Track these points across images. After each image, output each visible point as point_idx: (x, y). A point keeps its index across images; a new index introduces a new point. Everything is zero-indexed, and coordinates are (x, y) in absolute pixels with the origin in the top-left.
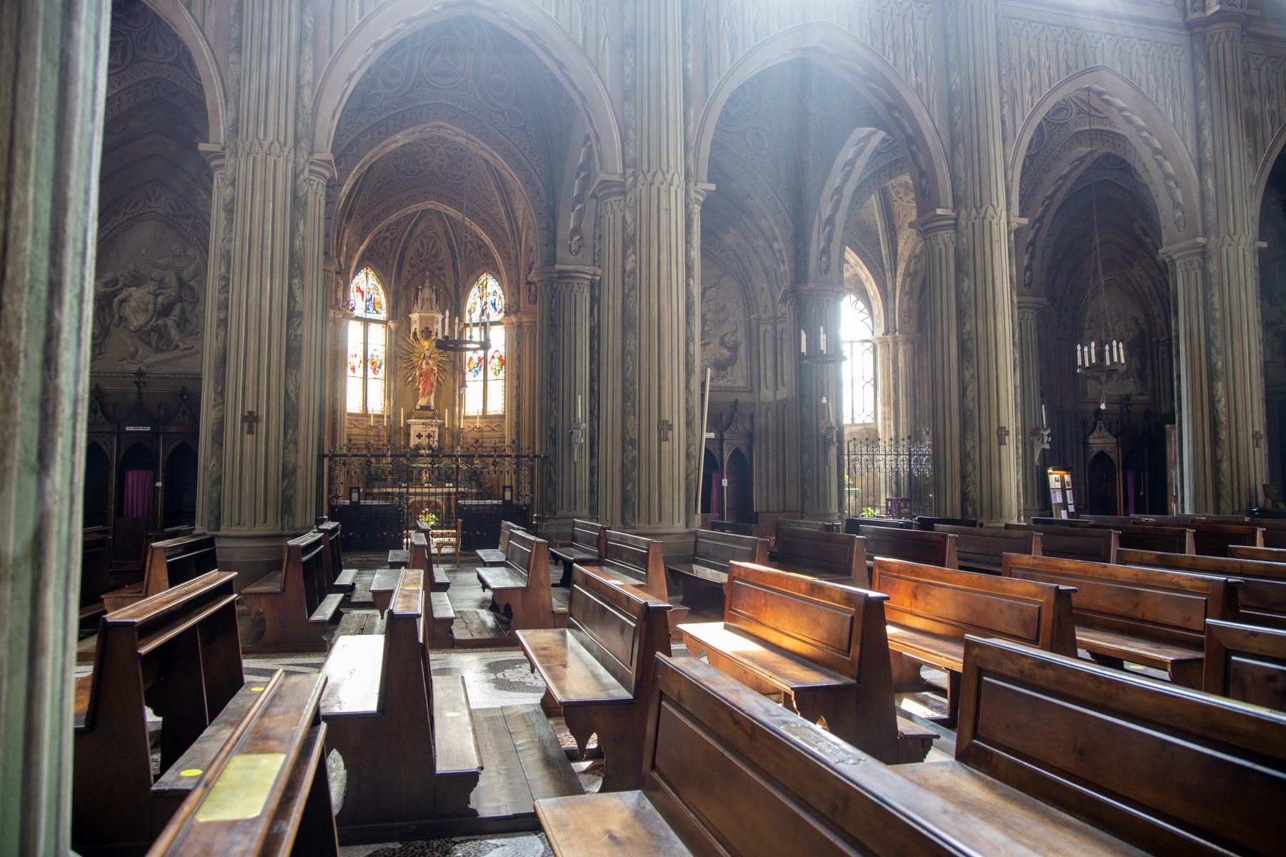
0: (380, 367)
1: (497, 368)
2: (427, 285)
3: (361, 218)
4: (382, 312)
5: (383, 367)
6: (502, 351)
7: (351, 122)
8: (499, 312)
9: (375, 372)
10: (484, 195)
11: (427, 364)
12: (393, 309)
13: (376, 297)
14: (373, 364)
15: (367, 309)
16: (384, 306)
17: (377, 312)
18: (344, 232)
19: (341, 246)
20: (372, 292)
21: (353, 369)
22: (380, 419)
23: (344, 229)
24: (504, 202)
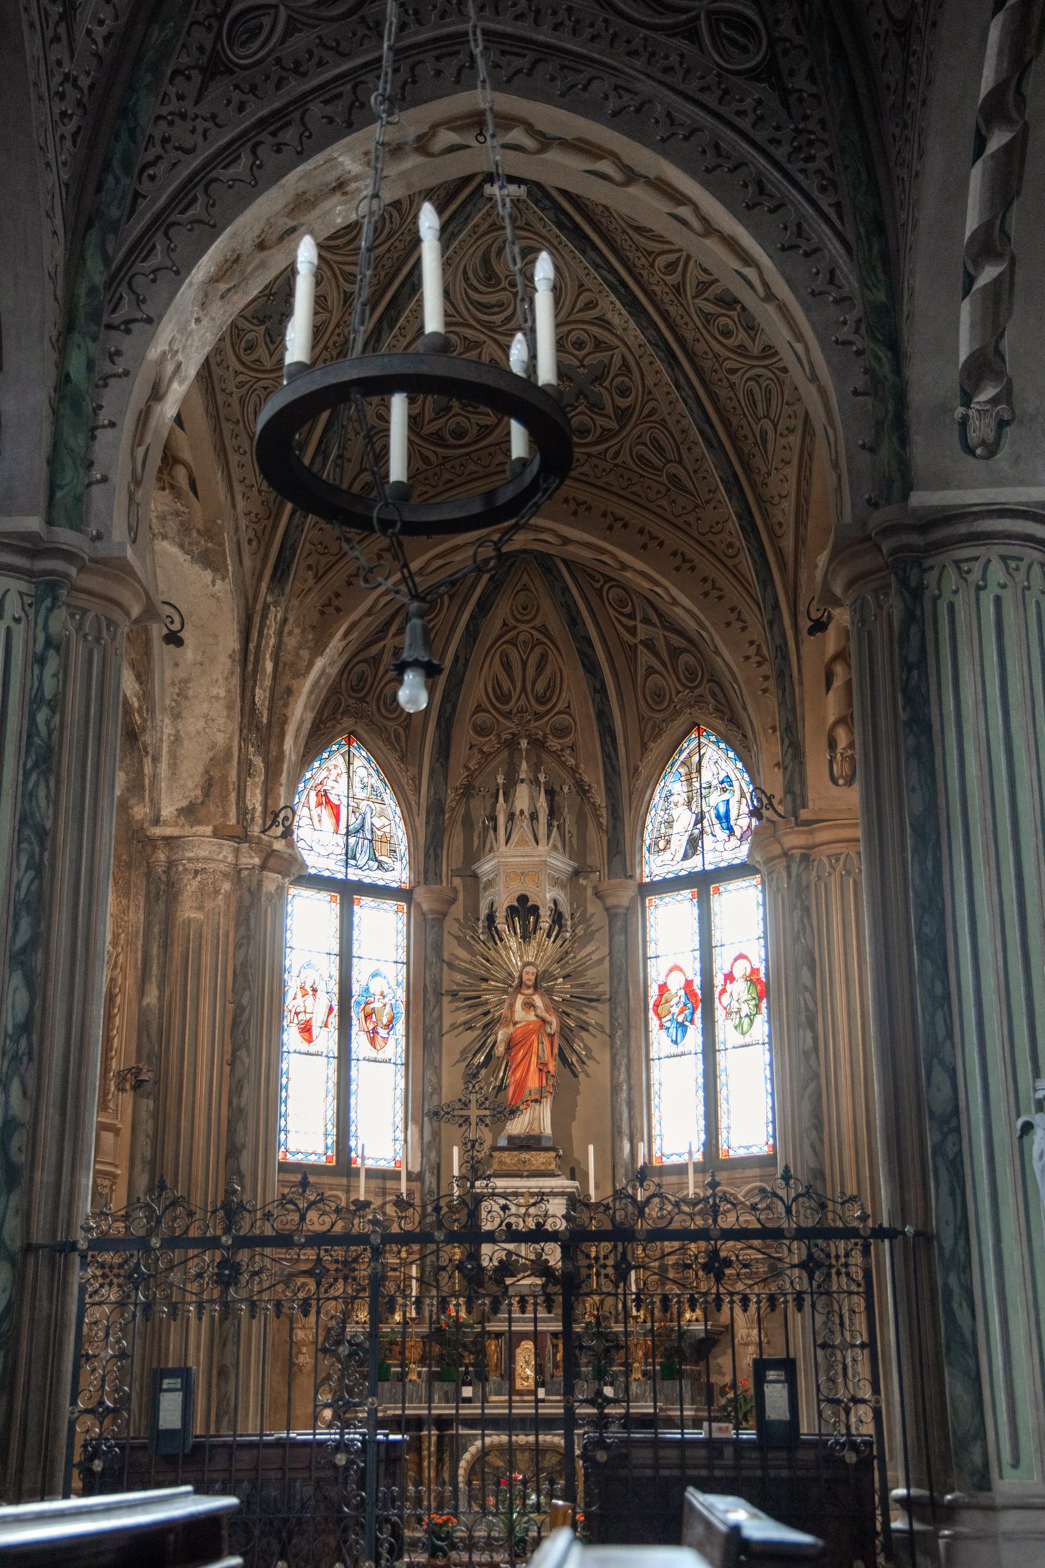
0: (389, 1026)
1: (745, 1010)
2: (523, 776)
3: (318, 578)
4: (398, 865)
5: (400, 1027)
6: (757, 955)
7: (183, 116)
9: (373, 1037)
10: (673, 478)
11: (529, 1005)
12: (427, 856)
13: (378, 822)
14: (368, 1016)
15: (350, 856)
16: (403, 848)
17: (381, 866)
18: (264, 617)
19: (256, 662)
21: (306, 1030)
22: (390, 1184)
23: (266, 607)
24: (733, 484)
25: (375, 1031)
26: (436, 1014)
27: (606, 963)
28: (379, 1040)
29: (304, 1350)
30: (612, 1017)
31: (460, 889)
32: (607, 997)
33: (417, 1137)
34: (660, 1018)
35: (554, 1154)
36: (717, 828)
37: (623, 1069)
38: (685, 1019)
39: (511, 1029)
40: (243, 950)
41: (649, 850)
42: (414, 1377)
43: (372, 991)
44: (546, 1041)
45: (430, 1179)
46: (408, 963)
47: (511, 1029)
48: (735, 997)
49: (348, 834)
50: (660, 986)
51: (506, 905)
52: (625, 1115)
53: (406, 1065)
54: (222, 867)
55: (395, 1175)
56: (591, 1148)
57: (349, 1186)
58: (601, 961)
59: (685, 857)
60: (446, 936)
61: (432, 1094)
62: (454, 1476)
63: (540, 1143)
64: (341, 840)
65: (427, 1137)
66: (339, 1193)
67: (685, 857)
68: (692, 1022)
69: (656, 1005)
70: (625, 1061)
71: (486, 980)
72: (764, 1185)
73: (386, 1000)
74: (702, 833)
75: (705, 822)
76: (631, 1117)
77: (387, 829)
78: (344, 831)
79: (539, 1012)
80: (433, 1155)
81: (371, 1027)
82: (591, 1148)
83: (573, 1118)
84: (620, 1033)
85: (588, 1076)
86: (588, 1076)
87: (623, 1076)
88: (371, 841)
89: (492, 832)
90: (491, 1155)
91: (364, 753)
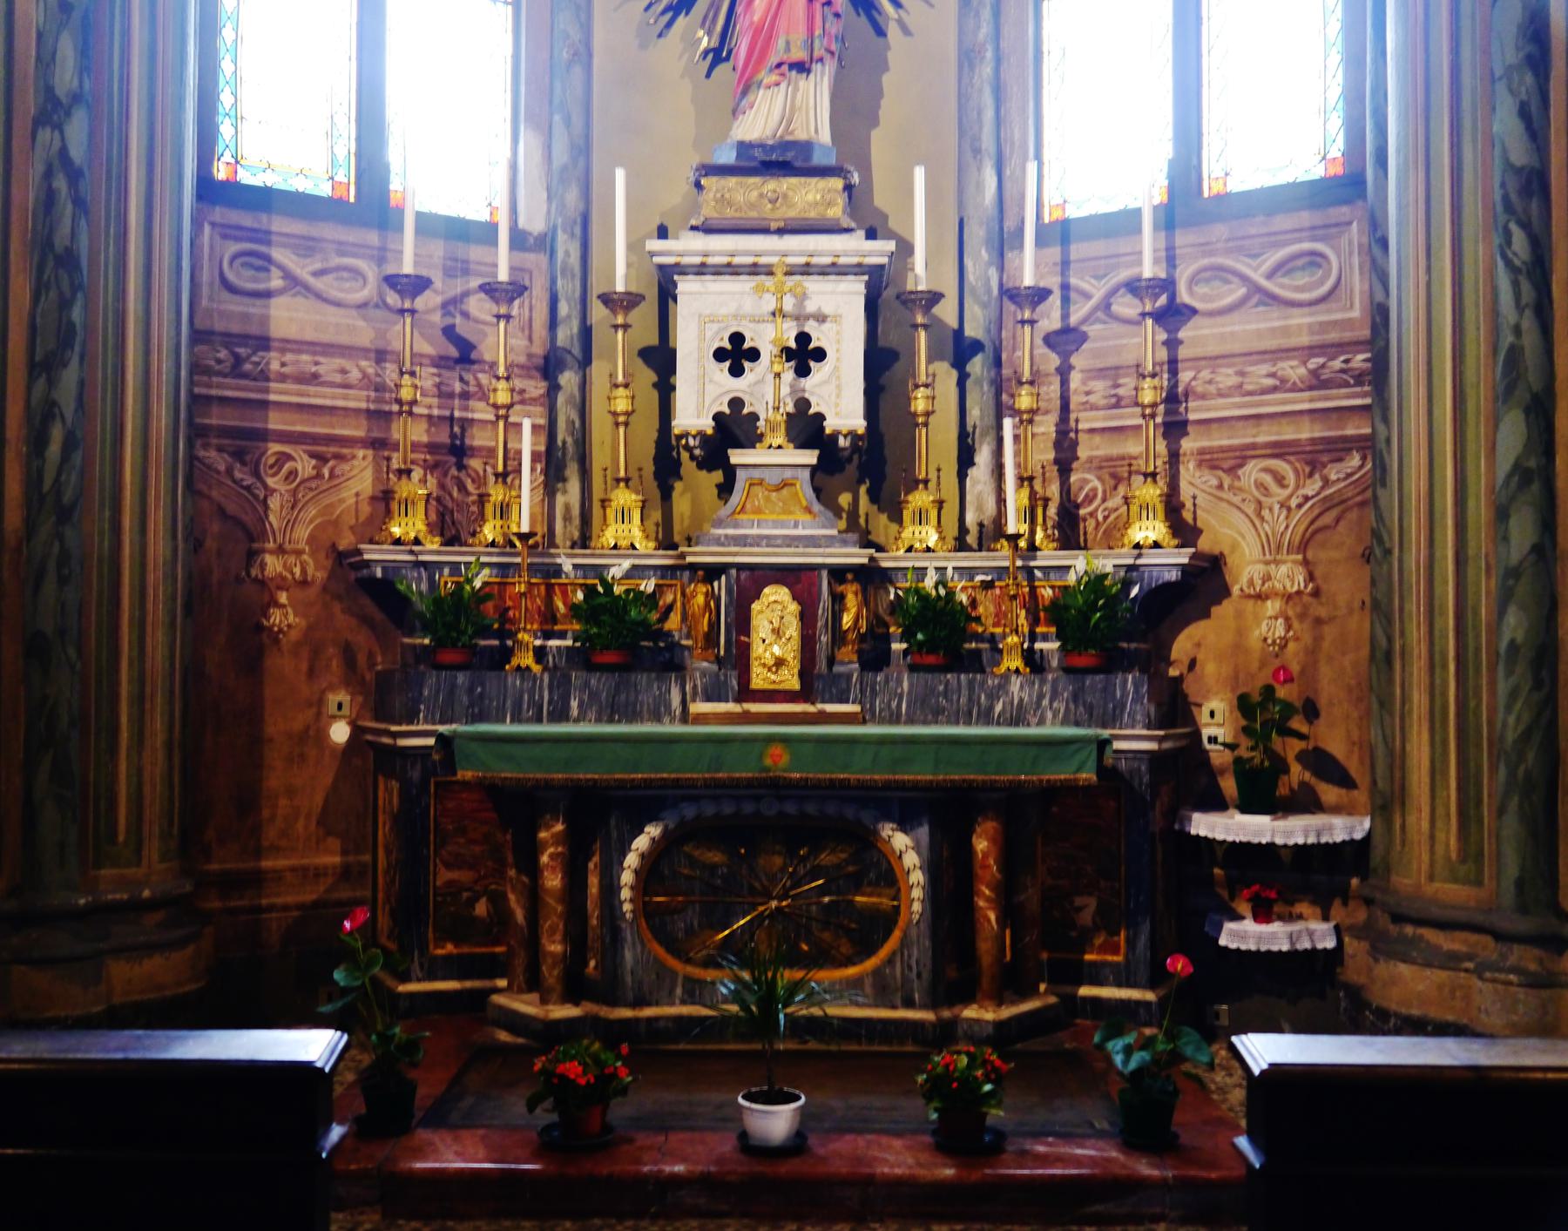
22: (476, 253)
33: (537, 156)
35: (838, 183)
45: (567, 248)
52: (989, 114)
55: (487, 232)
56: (919, 174)
57: (383, 249)
62: (610, 888)
63: (808, 157)
65: (561, 155)
66: (361, 264)
72: (1319, 247)
76: (999, 121)
80: (572, 197)
82: (919, 174)
83: (875, 122)
85: (906, 31)
86: (906, 31)
87: (985, 31)
90: (698, 185)
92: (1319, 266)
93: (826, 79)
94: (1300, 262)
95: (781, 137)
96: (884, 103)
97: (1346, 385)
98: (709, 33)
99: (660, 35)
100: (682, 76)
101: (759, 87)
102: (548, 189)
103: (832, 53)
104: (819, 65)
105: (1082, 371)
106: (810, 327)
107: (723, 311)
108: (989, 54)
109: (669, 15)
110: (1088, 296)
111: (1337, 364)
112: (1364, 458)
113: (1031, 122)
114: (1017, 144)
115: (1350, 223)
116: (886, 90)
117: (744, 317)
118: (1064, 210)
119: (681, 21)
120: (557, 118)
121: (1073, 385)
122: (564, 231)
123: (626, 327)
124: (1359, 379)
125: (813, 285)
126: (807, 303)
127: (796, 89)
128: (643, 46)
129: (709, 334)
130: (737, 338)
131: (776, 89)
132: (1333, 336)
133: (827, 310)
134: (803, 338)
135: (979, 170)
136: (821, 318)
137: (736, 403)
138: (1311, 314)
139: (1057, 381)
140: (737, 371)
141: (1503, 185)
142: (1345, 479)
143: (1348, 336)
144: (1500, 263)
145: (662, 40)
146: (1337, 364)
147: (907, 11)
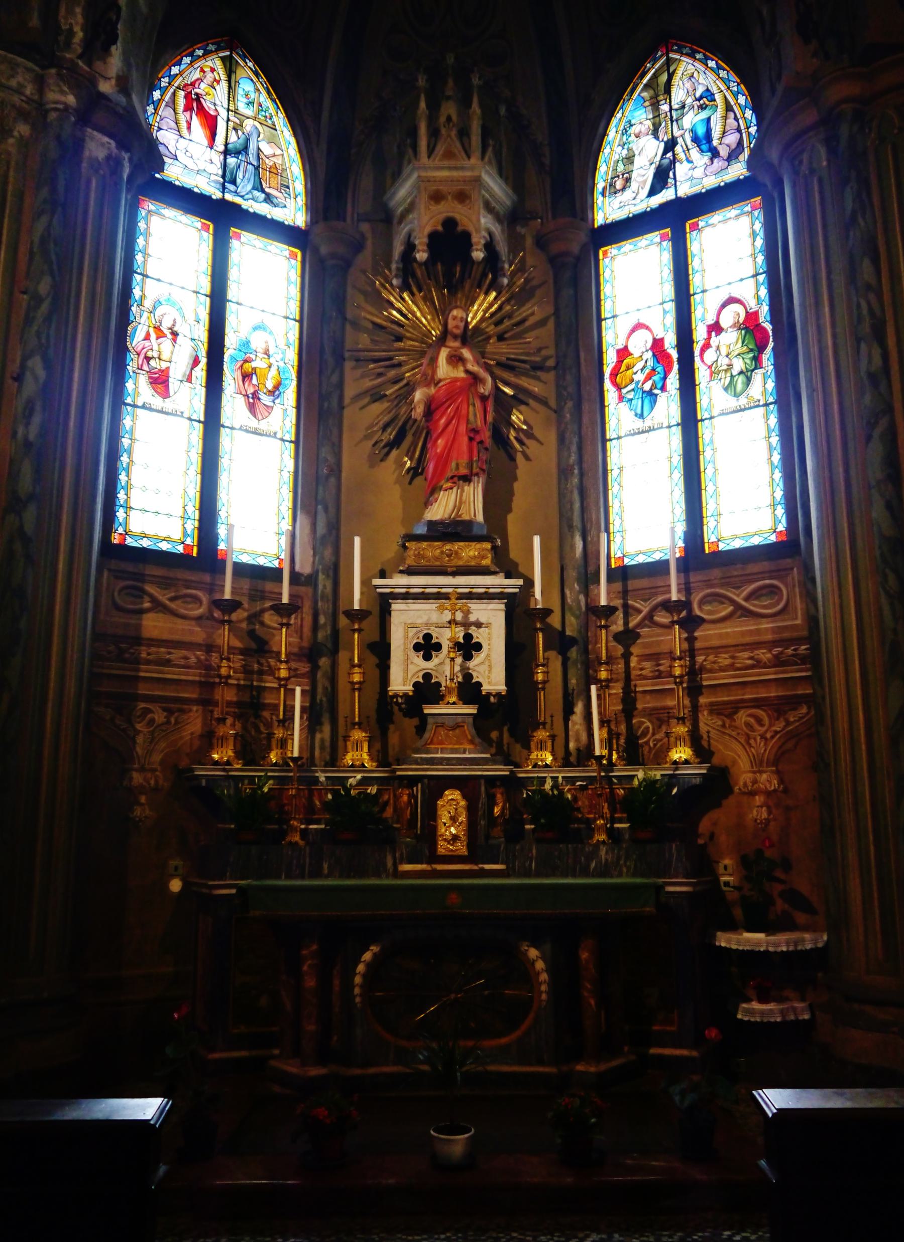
0: (275, 391)
1: (739, 365)
2: (449, 92)
4: (290, 203)
5: (290, 395)
8: (732, 156)
9: (253, 403)
11: (456, 359)
13: (267, 149)
14: (246, 376)
15: (228, 178)
16: (299, 185)
17: (268, 199)
20: (249, 124)
21: (160, 381)
22: (269, 586)
25: (255, 396)
26: (335, 378)
27: (551, 324)
28: (259, 408)
29: (143, 799)
30: (558, 386)
31: (369, 235)
32: (551, 363)
33: (307, 530)
34: (619, 388)
35: (488, 546)
36: (694, 153)
37: (574, 448)
38: (654, 386)
39: (433, 390)
40: (44, 219)
41: (603, 194)
42: (297, 838)
43: (253, 345)
44: (478, 404)
45: (324, 583)
46: (301, 321)
47: (433, 390)
48: (724, 351)
49: (226, 152)
50: (619, 352)
51: (428, 230)
52: (577, 506)
53: (296, 442)
54: (16, 99)
55: (275, 573)
56: (537, 540)
57: (212, 584)
58: (542, 323)
59: (652, 192)
60: (350, 291)
61: (327, 477)
63: (471, 530)
64: (218, 159)
65: (321, 529)
67: (652, 192)
68: (663, 388)
69: (614, 374)
70: (575, 440)
71: (399, 339)
73: (272, 360)
74: (674, 161)
75: (678, 149)
77: (278, 161)
78: (221, 148)
79: (470, 367)
80: (328, 553)
81: (251, 390)
82: (537, 540)
83: (510, 510)
84: (570, 404)
85: (527, 458)
86: (527, 458)
87: (573, 458)
88: (257, 168)
89: (410, 151)
90: (404, 547)
91: (250, 64)
92: (776, 593)
93: (480, 485)
94: (764, 592)
95: (454, 518)
96: (515, 498)
97: (796, 664)
98: (411, 459)
99: (382, 460)
100: (395, 483)
101: (440, 490)
102: (314, 549)
103: (483, 470)
104: (476, 478)
105: (637, 656)
106: (472, 630)
107: (419, 621)
108: (576, 471)
109: (386, 449)
110: (639, 611)
111: (790, 651)
112: (809, 708)
113: (602, 510)
114: (594, 522)
115: (792, 569)
116: (516, 493)
117: (432, 624)
118: (623, 561)
119: (394, 453)
120: (320, 507)
121: (632, 665)
122: (323, 574)
123: (359, 631)
124: (803, 660)
125: (474, 605)
126: (470, 616)
127: (463, 491)
128: (372, 465)
129: (411, 635)
130: (428, 637)
131: (451, 491)
132: (786, 635)
133: (482, 620)
134: (468, 637)
135: (573, 537)
136: (479, 625)
137: (427, 676)
138: (772, 622)
139: (622, 662)
140: (427, 658)
141: (880, 547)
142: (798, 721)
143: (796, 634)
144: (882, 593)
145: (383, 464)
146: (790, 651)
147: (528, 448)
